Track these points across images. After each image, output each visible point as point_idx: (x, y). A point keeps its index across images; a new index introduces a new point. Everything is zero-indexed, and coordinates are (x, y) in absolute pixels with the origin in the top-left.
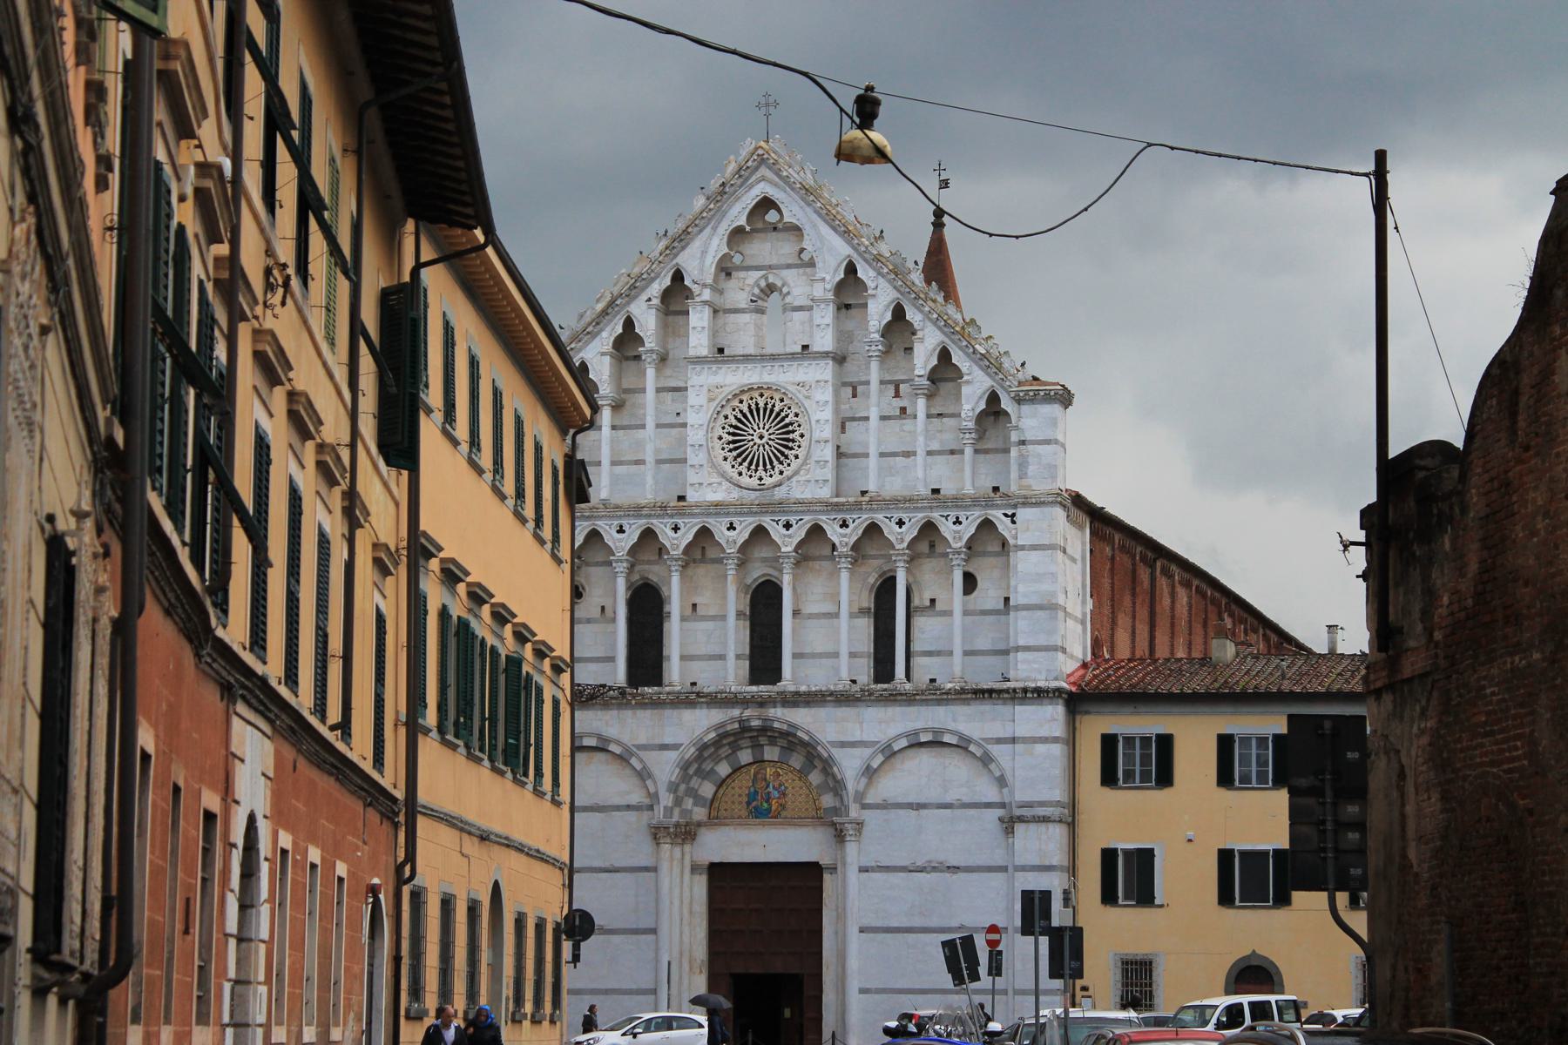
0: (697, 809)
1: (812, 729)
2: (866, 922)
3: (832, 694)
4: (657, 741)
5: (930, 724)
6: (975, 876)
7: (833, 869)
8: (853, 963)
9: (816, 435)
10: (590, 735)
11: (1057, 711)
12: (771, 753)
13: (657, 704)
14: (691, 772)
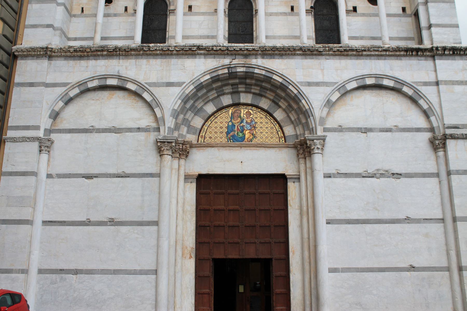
2: (331, 216)
3: (301, 49)
4: (165, 80)
5: (374, 72)
6: (414, 180)
8: (324, 249)
13: (167, 53)
14: (188, 106)
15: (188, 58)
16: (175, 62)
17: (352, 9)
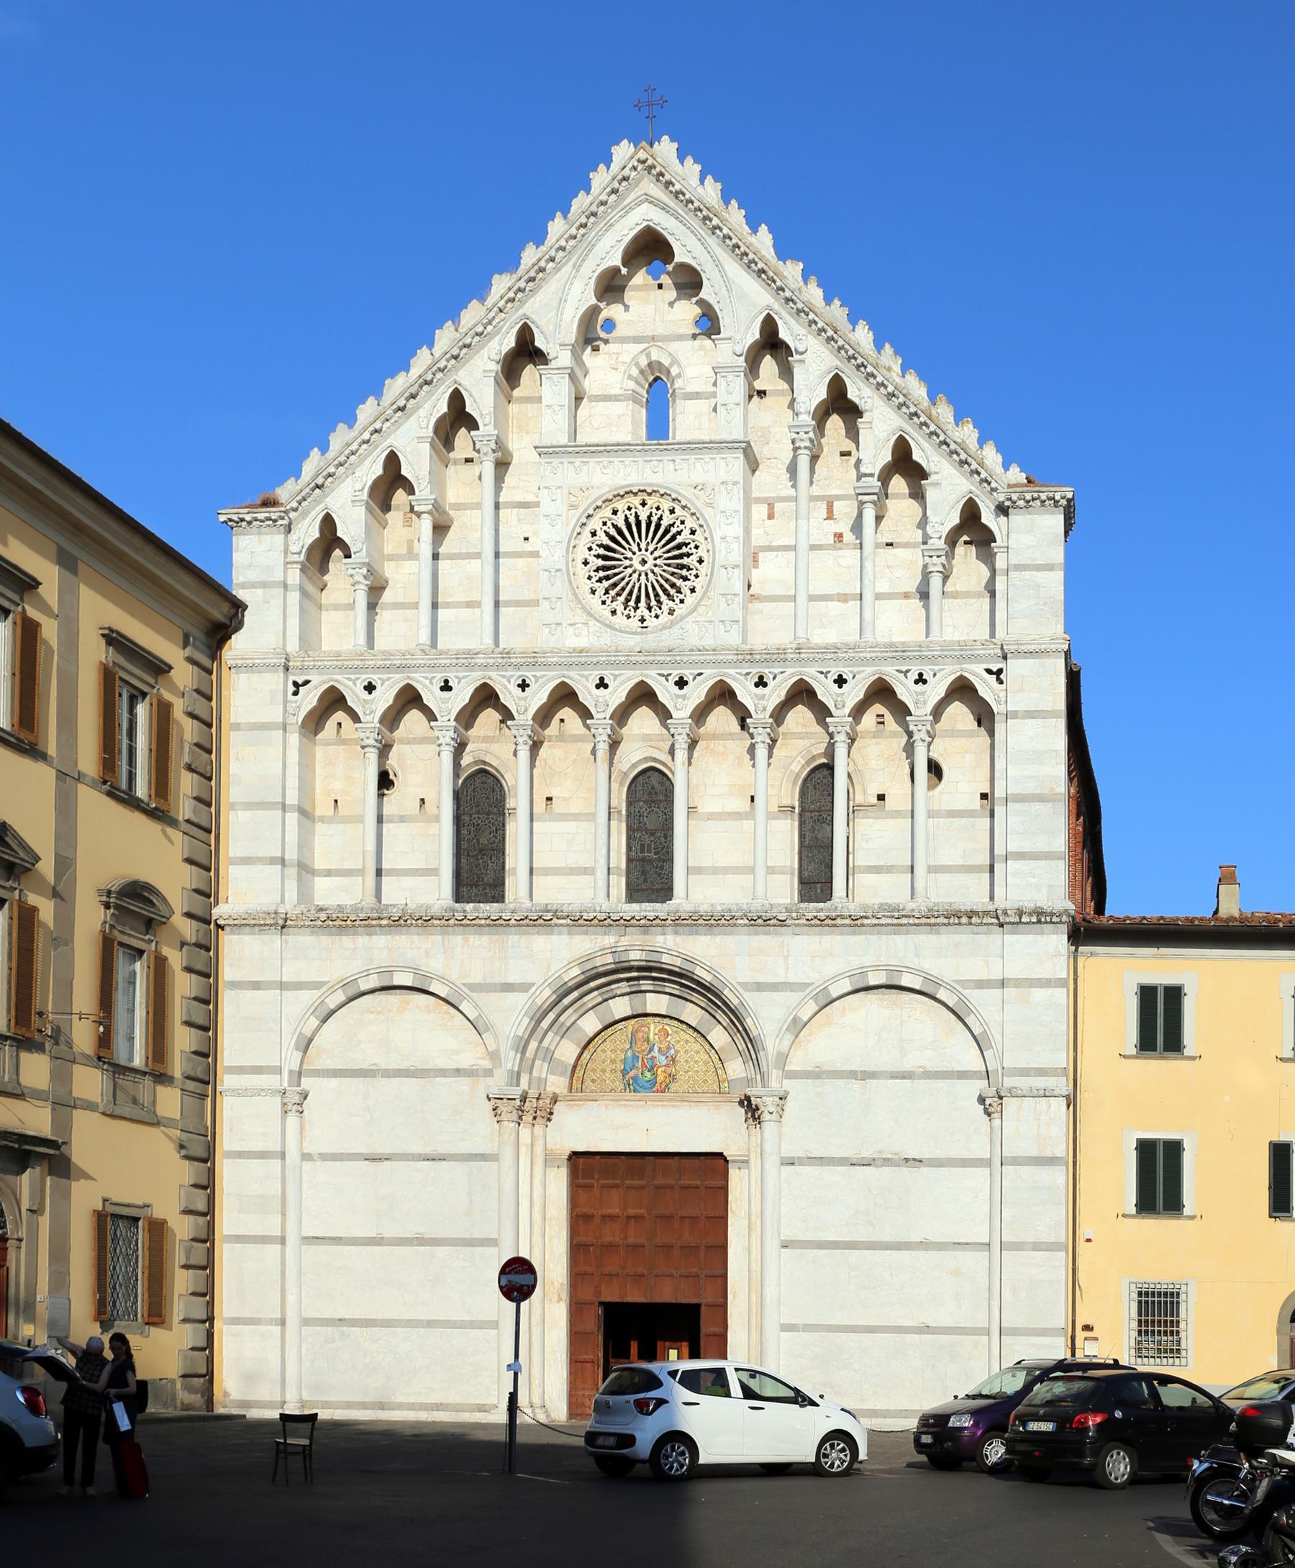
0: (551, 1078)
1: (715, 964)
5: (884, 960)
9: (720, 559)
10: (404, 969)
11: (1058, 940)
15: (538, 933)
16: (515, 940)
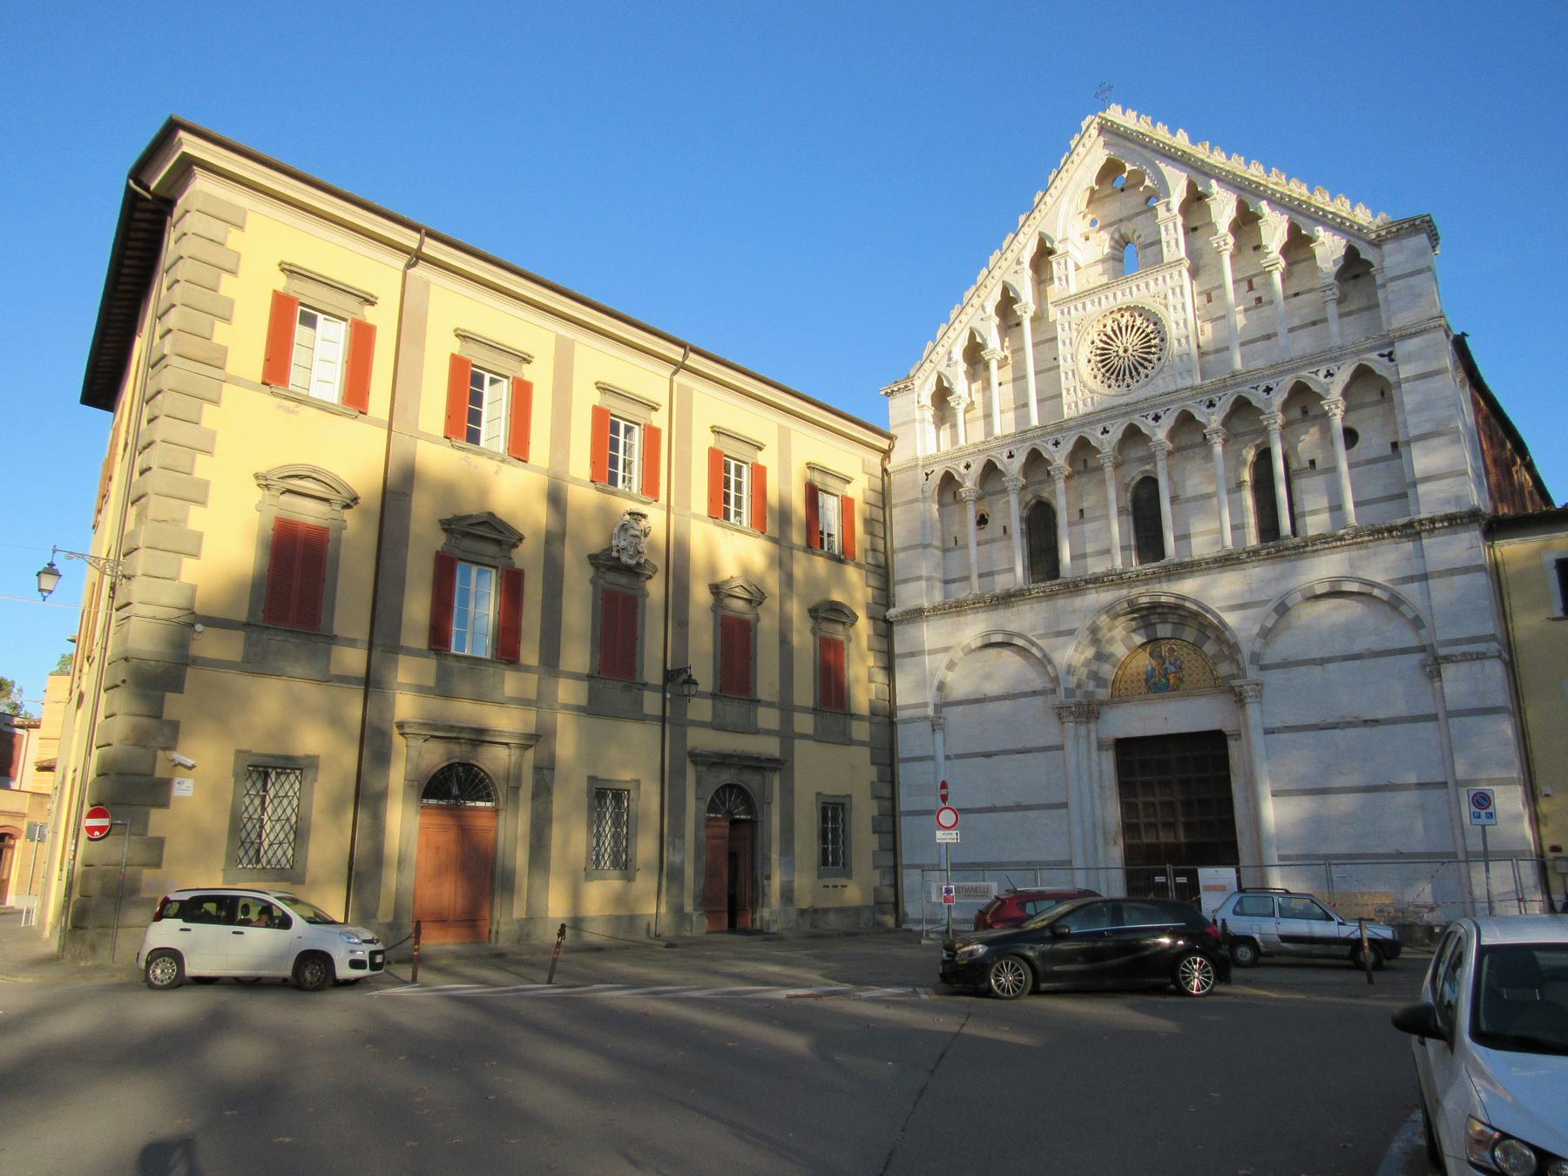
0: (1099, 691)
6: (1399, 728)
7: (1238, 736)
12: (1164, 630)
17: (1307, 465)
